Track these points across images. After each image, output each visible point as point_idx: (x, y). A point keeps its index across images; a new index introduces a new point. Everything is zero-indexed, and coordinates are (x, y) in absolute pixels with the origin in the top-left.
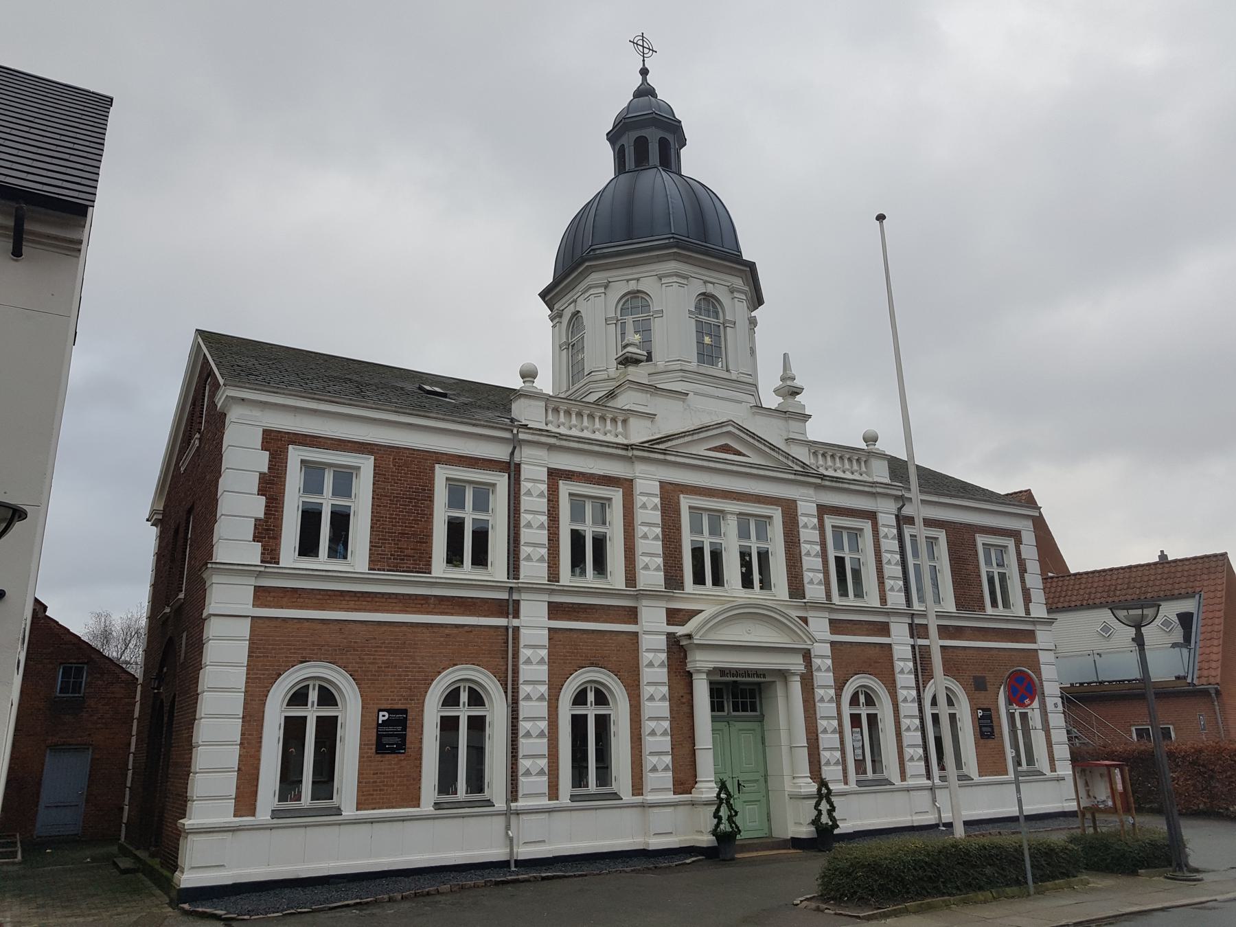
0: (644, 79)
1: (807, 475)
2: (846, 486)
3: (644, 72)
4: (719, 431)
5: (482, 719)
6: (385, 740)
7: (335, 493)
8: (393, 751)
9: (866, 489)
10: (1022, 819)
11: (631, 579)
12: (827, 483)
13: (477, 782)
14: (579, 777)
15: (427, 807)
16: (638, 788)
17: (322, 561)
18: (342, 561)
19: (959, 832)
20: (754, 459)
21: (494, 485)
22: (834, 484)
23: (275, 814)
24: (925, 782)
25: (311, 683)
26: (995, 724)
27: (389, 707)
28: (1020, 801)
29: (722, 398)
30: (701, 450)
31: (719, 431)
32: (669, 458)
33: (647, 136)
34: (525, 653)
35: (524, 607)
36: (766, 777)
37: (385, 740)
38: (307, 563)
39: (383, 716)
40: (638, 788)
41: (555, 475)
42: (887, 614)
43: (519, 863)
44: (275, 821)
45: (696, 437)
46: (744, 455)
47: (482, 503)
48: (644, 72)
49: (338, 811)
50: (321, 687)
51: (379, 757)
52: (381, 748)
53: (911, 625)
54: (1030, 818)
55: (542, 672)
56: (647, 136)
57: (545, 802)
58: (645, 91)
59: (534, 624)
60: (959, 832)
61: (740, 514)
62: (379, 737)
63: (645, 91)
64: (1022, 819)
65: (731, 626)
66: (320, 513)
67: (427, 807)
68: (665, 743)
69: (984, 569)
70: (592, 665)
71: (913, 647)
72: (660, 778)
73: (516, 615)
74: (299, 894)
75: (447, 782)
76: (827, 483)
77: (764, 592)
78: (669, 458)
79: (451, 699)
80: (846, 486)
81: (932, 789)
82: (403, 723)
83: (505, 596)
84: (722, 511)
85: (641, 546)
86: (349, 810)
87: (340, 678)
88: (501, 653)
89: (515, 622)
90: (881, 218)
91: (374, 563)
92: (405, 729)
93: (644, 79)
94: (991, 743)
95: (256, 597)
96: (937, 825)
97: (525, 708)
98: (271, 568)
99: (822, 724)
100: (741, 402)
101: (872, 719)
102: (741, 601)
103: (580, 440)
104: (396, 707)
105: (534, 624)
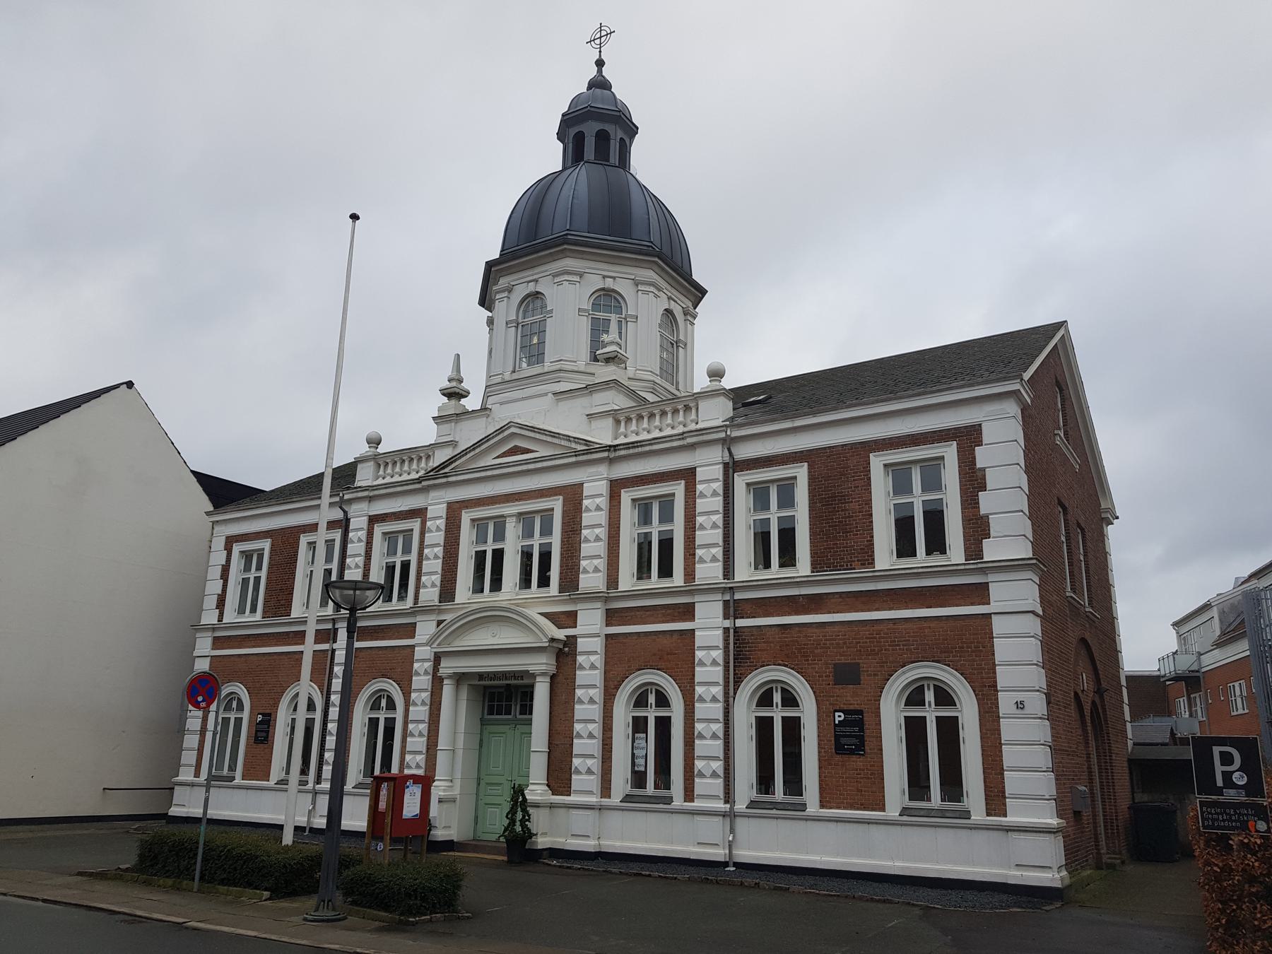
0: (600, 71)
1: (588, 452)
2: (647, 448)
3: (600, 63)
4: (501, 436)
5: (797, 720)
6: (843, 741)
7: (925, 489)
8: (852, 752)
9: (675, 444)
10: (204, 821)
11: (690, 574)
12: (623, 453)
13: (794, 783)
14: (765, 781)
15: (892, 811)
16: (689, 795)
17: (655, 582)
18: (943, 557)
19: (288, 838)
20: (543, 452)
21: (943, 458)
22: (631, 451)
23: (905, 811)
24: (720, 805)
25: (926, 683)
26: (867, 733)
27: (845, 708)
28: (207, 800)
29: (523, 399)
30: (489, 461)
31: (501, 436)
32: (451, 479)
33: (597, 130)
34: (718, 654)
35: (699, 609)
36: (479, 779)
37: (843, 741)
38: (479, 598)
39: (839, 717)
40: (689, 795)
41: (689, 475)
42: (983, 571)
43: (738, 865)
44: (905, 818)
45: (477, 451)
46: (533, 451)
47: (933, 481)
48: (600, 63)
49: (803, 807)
50: (657, 691)
51: (838, 758)
52: (840, 749)
53: (726, 603)
54: (212, 822)
55: (717, 673)
56: (597, 130)
57: (593, 800)
58: (600, 83)
59: (709, 626)
60: (288, 838)
61: (520, 514)
62: (837, 738)
63: (600, 83)
64: (204, 821)
65: (512, 631)
66: (672, 540)
67: (892, 811)
68: (579, 745)
69: (263, 574)
70: (384, 676)
71: (726, 630)
72: (707, 786)
73: (692, 618)
74: (810, 880)
75: (917, 785)
76: (623, 453)
77: (542, 589)
78: (451, 479)
79: (915, 698)
80: (647, 448)
81: (731, 816)
82: (860, 724)
83: (329, 626)
84: (502, 516)
85: (601, 548)
86: (813, 808)
87: (954, 680)
88: (971, 649)
89: (727, 623)
90: (354, 217)
91: (816, 565)
92: (862, 730)
93: (600, 71)
94: (856, 762)
95: (214, 643)
96: (726, 864)
97: (700, 709)
98: (613, 593)
99: (423, 727)
100: (546, 394)
101: (664, 725)
102: (475, 607)
103: (386, 486)
104: (852, 707)
105: (709, 626)
